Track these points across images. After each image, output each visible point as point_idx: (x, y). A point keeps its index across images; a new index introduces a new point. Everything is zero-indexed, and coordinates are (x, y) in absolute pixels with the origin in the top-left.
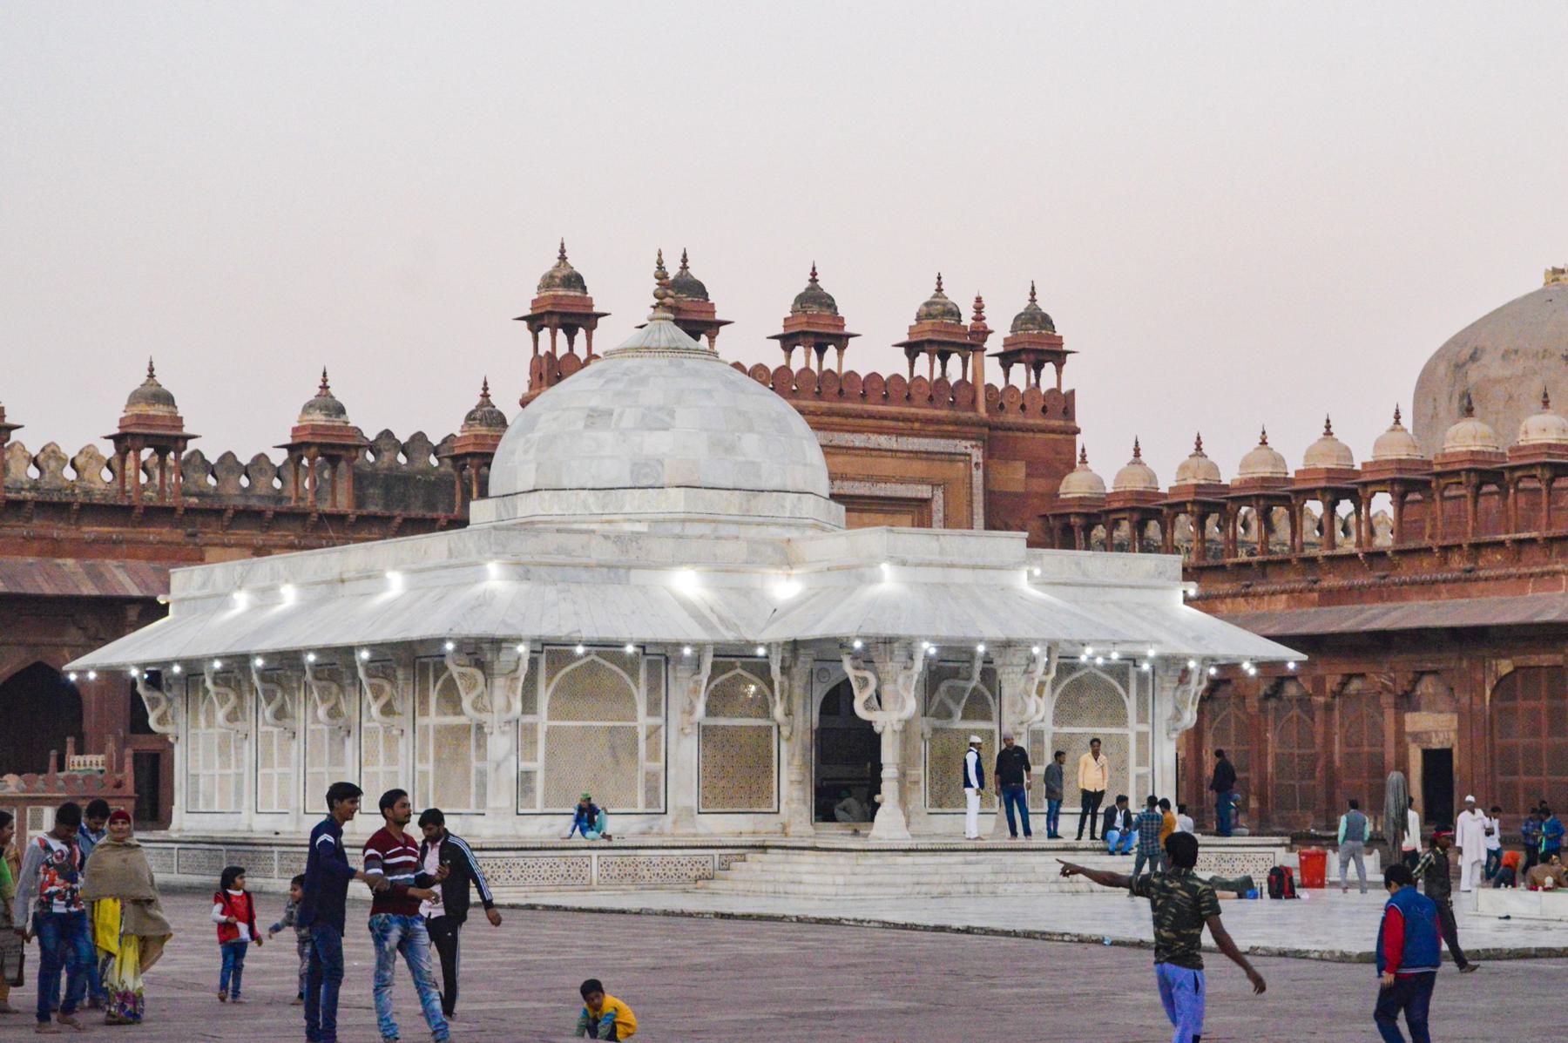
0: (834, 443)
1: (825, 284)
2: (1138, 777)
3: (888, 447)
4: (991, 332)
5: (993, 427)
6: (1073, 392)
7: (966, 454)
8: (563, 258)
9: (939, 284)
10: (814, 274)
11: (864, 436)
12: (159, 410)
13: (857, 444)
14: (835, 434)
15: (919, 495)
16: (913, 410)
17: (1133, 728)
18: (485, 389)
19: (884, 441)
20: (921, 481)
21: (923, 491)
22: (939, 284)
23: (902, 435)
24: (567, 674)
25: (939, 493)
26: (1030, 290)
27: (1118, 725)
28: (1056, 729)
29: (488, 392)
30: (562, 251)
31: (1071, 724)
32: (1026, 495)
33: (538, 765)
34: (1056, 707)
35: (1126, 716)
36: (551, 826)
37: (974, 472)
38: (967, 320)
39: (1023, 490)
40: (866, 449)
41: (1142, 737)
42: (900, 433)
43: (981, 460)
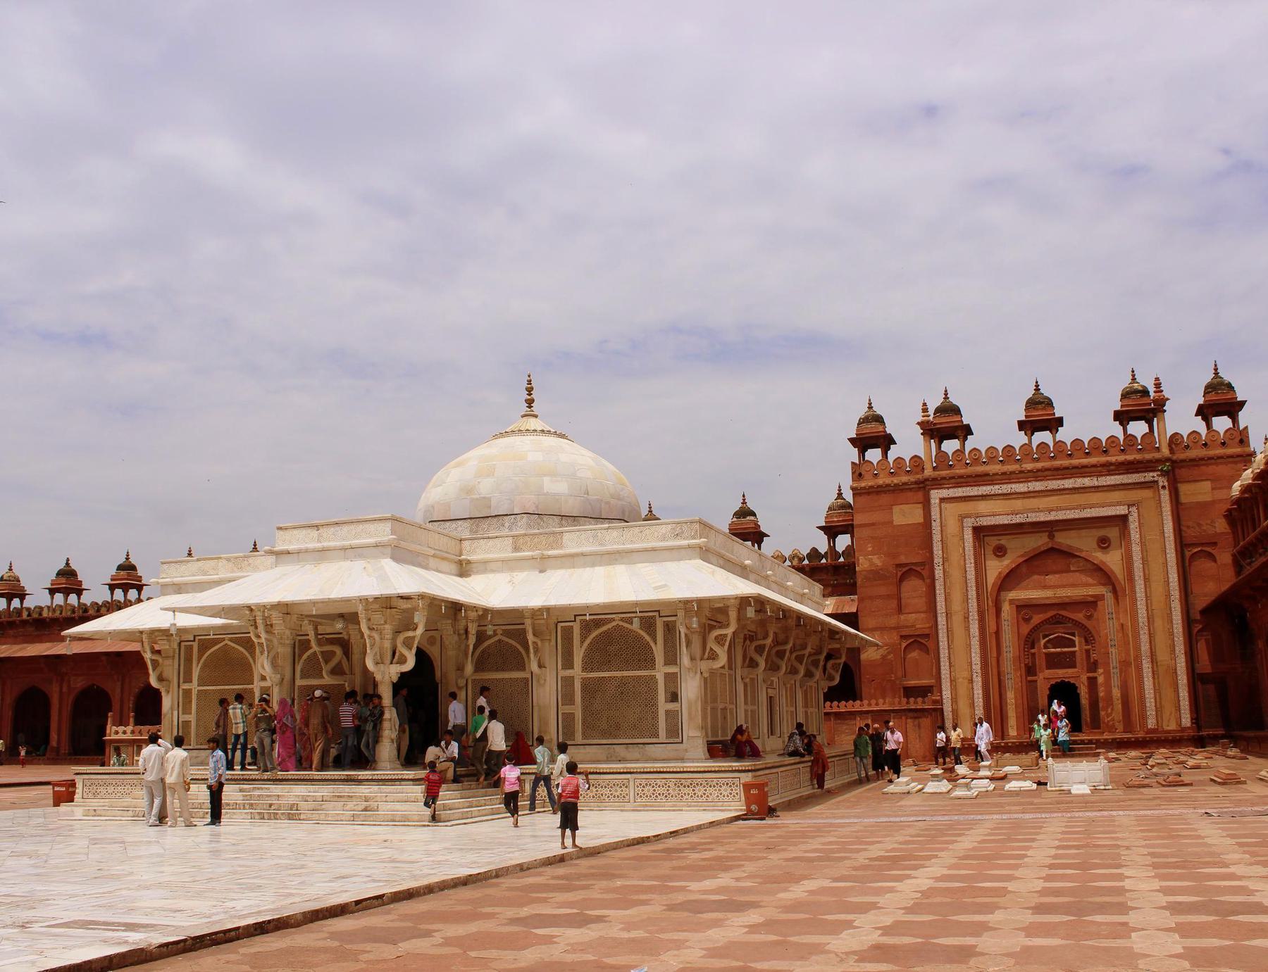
0: (1048, 488)
1: (1045, 391)
2: (666, 711)
3: (1091, 485)
4: (1168, 399)
5: (1173, 462)
6: (1246, 427)
7: (1157, 482)
8: (870, 407)
9: (1133, 376)
10: (1037, 386)
11: (1072, 481)
13: (1066, 486)
14: (1049, 482)
15: (1118, 513)
16: (1109, 459)
18: (840, 490)
19: (1087, 482)
20: (1119, 504)
21: (1122, 510)
22: (1133, 376)
23: (1102, 476)
24: (212, 653)
25: (1134, 509)
26: (1213, 367)
27: (646, 668)
28: (585, 675)
29: (842, 491)
30: (870, 404)
31: (599, 670)
32: (1213, 502)
33: (192, 718)
34: (586, 656)
35: (653, 660)
36: (196, 757)
37: (1162, 492)
38: (1152, 394)
39: (1211, 499)
40: (1075, 489)
42: (1100, 475)
43: (1166, 484)
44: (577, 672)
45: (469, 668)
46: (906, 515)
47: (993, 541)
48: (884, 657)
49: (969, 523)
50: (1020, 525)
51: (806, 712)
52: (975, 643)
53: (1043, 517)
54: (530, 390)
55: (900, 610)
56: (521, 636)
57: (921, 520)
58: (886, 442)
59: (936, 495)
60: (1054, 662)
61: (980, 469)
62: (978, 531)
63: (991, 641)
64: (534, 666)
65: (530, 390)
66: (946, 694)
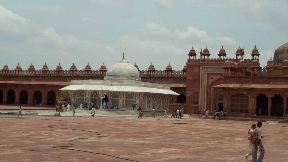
12: (170, 67)
17: (134, 100)
30: (193, 47)
41: (135, 100)
44: (125, 99)
45: (112, 97)
46: (196, 70)
47: (211, 76)
48: (190, 96)
49: (207, 72)
50: (215, 74)
51: (164, 105)
52: (206, 95)
53: (219, 73)
54: (124, 55)
55: (194, 87)
56: (118, 94)
57: (199, 71)
58: (195, 55)
59: (201, 67)
60: (220, 99)
61: (210, 62)
62: (208, 74)
63: (209, 94)
64: (119, 98)
65: (124, 55)
66: (200, 103)
